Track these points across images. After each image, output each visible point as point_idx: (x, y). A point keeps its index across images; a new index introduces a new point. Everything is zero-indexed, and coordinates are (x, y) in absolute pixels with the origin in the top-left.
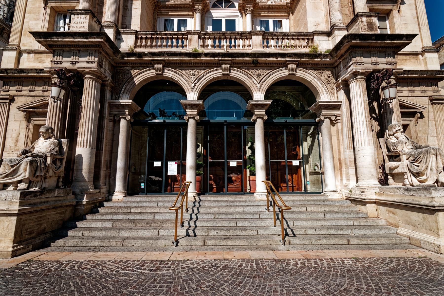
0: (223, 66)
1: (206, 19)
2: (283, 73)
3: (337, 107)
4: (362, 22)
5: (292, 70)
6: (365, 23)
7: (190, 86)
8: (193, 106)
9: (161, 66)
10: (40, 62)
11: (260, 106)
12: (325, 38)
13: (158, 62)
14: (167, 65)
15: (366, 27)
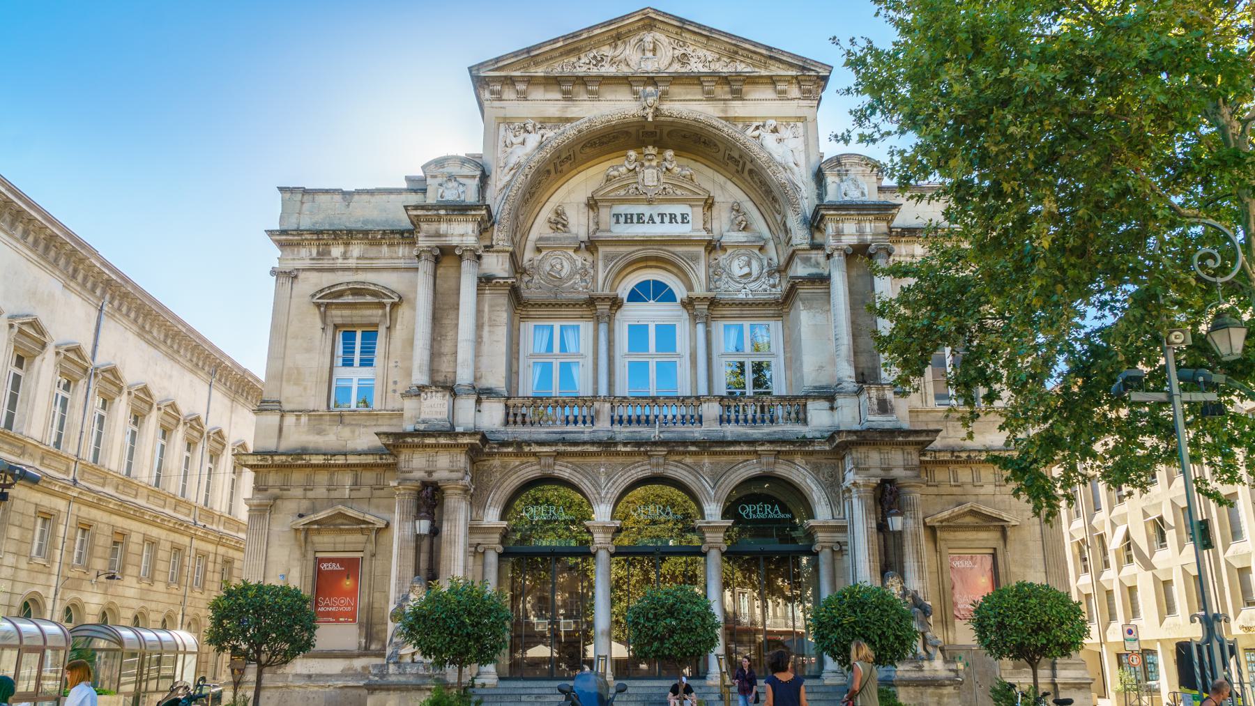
0: (654, 460)
1: (617, 323)
2: (751, 469)
3: (842, 529)
4: (870, 398)
5: (768, 464)
6: (875, 401)
7: (599, 494)
8: (605, 529)
9: (551, 461)
10: (319, 434)
11: (715, 529)
12: (826, 404)
13: (548, 455)
14: (559, 454)
15: (876, 407)
